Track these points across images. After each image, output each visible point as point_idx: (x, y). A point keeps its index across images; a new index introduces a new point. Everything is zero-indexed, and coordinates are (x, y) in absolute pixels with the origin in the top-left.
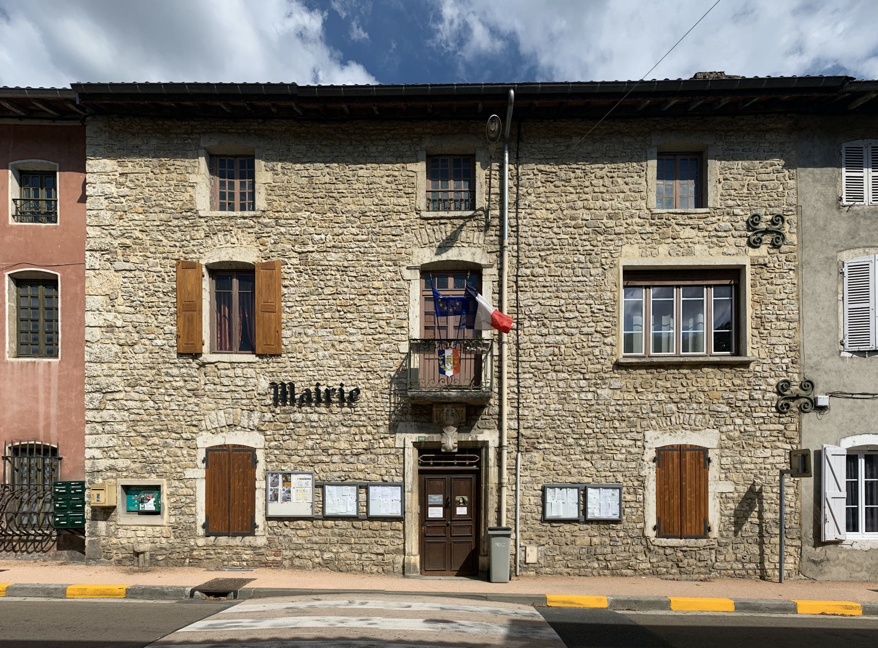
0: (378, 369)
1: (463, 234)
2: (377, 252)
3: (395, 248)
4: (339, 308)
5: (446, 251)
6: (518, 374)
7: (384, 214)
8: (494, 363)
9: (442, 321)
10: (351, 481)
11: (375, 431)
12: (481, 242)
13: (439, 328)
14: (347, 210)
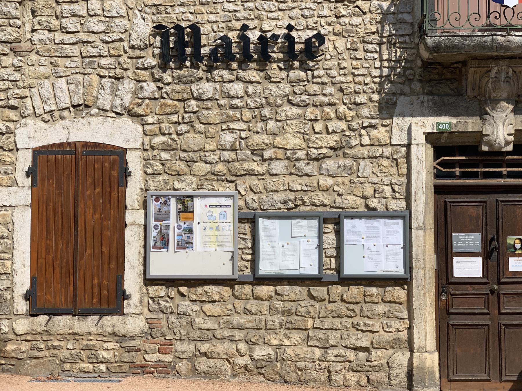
10: (307, 209)
11: (353, 114)
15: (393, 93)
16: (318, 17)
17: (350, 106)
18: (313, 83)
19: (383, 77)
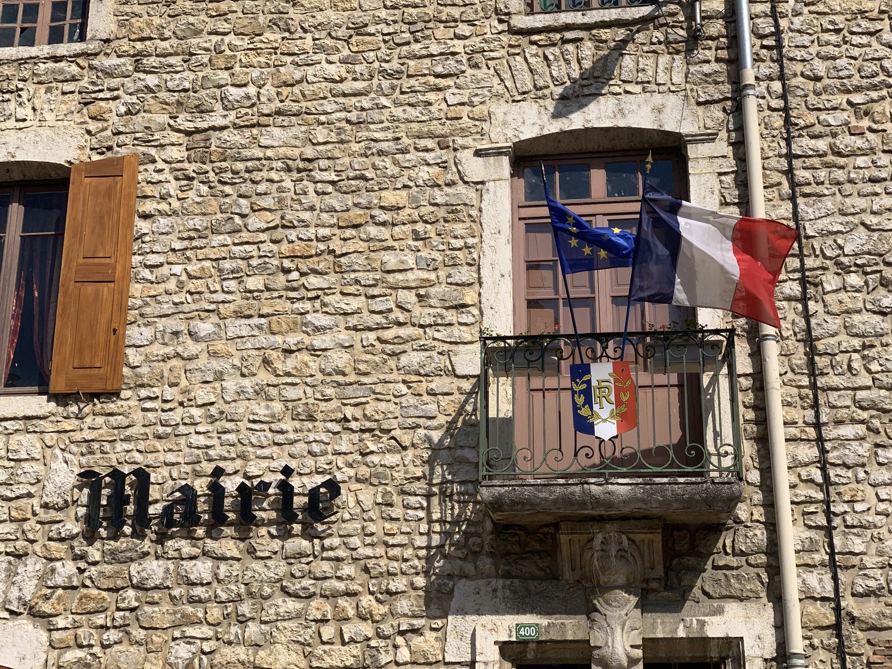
0: (394, 424)
1: (628, 62)
2: (394, 120)
3: (444, 106)
4: (287, 264)
5: (581, 106)
6: (818, 425)
7: (413, 28)
8: (740, 396)
9: (578, 284)
11: (384, 609)
12: (678, 78)
13: (570, 302)
14: (316, 23)
15: (449, 575)
16: (333, 454)
17: (379, 596)
18: (323, 559)
19: (433, 548)
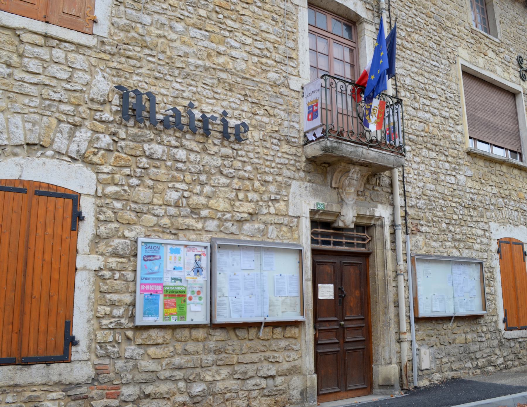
0: (266, 103)
4: (217, 9)
11: (264, 189)
